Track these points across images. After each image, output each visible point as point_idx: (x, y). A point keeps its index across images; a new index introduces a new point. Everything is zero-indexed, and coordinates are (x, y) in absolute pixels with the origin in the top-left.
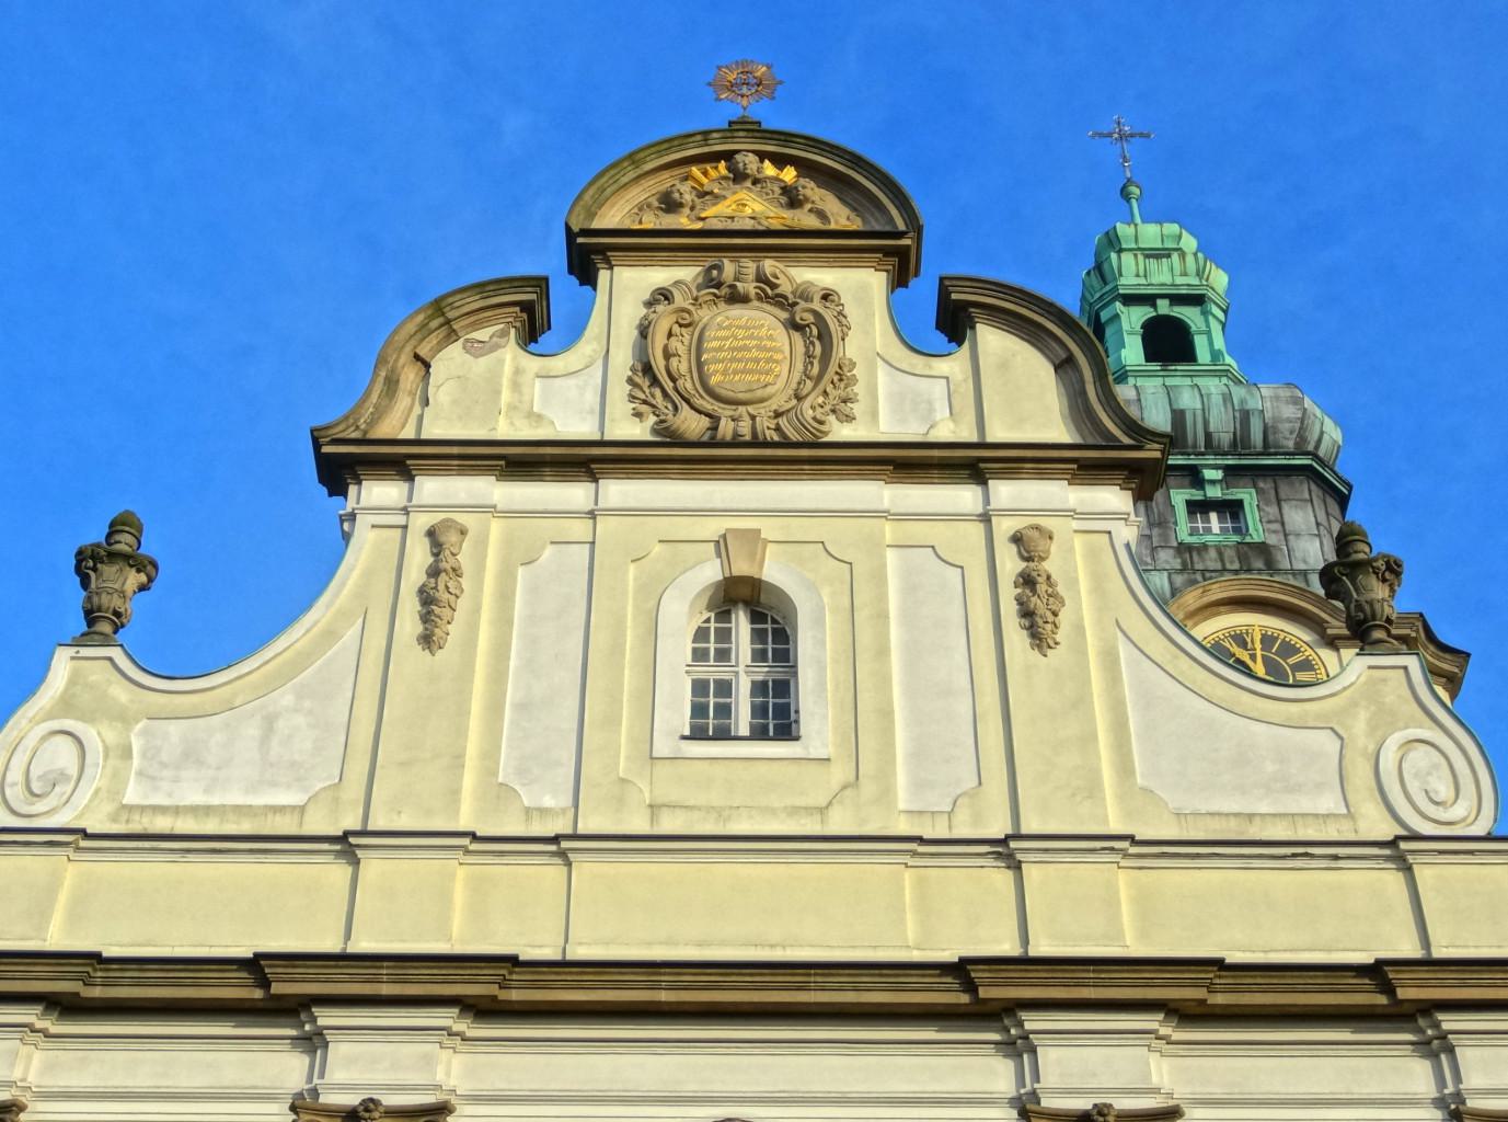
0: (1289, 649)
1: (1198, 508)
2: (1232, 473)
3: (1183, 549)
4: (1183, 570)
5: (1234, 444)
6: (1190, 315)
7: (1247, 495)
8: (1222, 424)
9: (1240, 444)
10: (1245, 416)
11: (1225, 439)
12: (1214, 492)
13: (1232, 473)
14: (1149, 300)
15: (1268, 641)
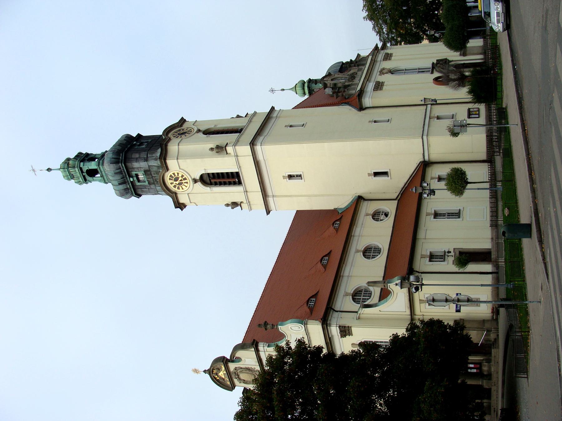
0: (171, 176)
1: (139, 181)
2: (130, 176)
3: (149, 183)
4: (154, 183)
5: (122, 174)
6: (85, 170)
7: (134, 173)
8: (118, 177)
9: (121, 173)
10: (115, 173)
11: (121, 175)
12: (135, 178)
13: (130, 176)
14: (84, 177)
15: (170, 179)
